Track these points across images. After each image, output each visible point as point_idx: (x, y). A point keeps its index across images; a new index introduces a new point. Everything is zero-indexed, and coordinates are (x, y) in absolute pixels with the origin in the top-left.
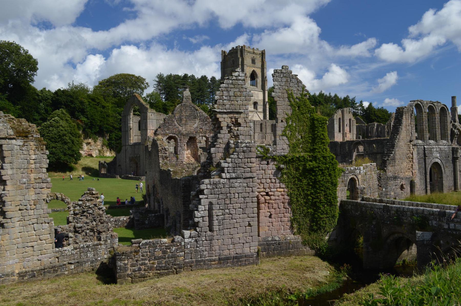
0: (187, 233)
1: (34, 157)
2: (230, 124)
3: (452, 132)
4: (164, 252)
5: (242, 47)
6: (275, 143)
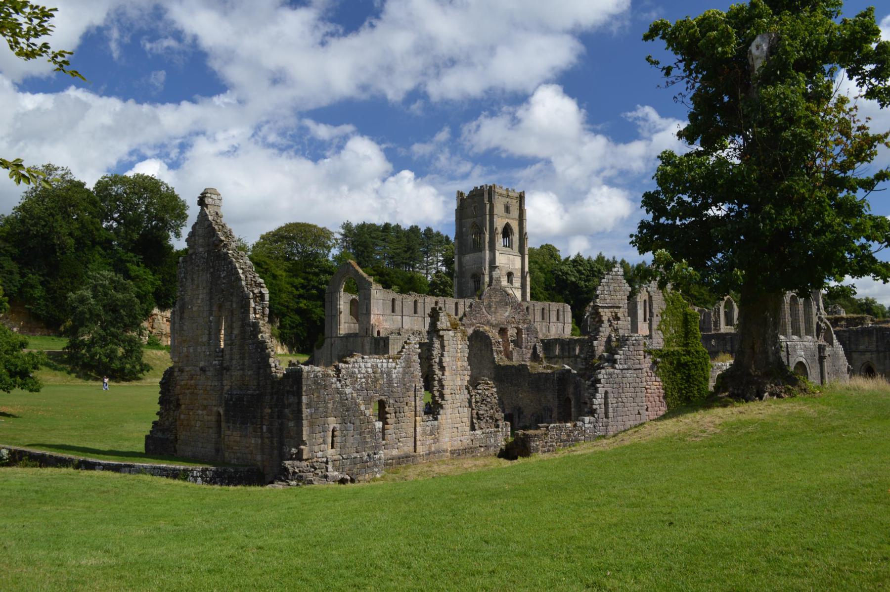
0: (587, 419)
1: (460, 347)
2: (611, 318)
3: (818, 326)
4: (568, 436)
5: (491, 187)
6: (650, 337)
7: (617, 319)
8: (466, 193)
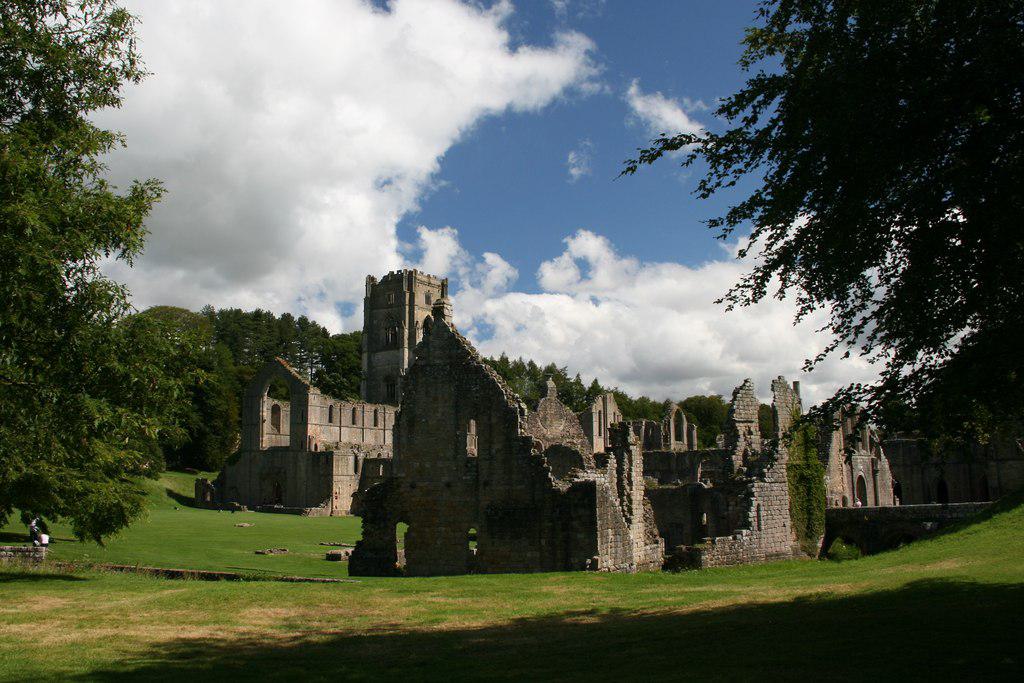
0: (744, 531)
3: (871, 440)
5: (411, 273)
7: (750, 433)
8: (379, 279)
